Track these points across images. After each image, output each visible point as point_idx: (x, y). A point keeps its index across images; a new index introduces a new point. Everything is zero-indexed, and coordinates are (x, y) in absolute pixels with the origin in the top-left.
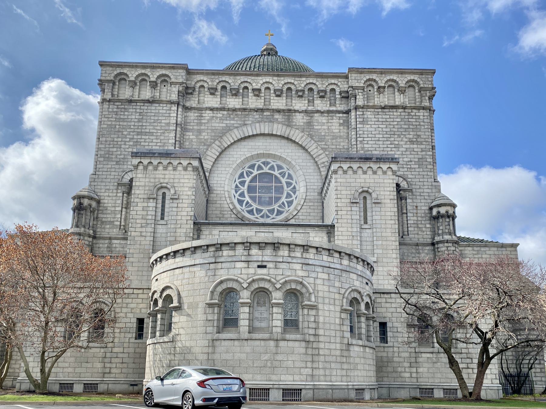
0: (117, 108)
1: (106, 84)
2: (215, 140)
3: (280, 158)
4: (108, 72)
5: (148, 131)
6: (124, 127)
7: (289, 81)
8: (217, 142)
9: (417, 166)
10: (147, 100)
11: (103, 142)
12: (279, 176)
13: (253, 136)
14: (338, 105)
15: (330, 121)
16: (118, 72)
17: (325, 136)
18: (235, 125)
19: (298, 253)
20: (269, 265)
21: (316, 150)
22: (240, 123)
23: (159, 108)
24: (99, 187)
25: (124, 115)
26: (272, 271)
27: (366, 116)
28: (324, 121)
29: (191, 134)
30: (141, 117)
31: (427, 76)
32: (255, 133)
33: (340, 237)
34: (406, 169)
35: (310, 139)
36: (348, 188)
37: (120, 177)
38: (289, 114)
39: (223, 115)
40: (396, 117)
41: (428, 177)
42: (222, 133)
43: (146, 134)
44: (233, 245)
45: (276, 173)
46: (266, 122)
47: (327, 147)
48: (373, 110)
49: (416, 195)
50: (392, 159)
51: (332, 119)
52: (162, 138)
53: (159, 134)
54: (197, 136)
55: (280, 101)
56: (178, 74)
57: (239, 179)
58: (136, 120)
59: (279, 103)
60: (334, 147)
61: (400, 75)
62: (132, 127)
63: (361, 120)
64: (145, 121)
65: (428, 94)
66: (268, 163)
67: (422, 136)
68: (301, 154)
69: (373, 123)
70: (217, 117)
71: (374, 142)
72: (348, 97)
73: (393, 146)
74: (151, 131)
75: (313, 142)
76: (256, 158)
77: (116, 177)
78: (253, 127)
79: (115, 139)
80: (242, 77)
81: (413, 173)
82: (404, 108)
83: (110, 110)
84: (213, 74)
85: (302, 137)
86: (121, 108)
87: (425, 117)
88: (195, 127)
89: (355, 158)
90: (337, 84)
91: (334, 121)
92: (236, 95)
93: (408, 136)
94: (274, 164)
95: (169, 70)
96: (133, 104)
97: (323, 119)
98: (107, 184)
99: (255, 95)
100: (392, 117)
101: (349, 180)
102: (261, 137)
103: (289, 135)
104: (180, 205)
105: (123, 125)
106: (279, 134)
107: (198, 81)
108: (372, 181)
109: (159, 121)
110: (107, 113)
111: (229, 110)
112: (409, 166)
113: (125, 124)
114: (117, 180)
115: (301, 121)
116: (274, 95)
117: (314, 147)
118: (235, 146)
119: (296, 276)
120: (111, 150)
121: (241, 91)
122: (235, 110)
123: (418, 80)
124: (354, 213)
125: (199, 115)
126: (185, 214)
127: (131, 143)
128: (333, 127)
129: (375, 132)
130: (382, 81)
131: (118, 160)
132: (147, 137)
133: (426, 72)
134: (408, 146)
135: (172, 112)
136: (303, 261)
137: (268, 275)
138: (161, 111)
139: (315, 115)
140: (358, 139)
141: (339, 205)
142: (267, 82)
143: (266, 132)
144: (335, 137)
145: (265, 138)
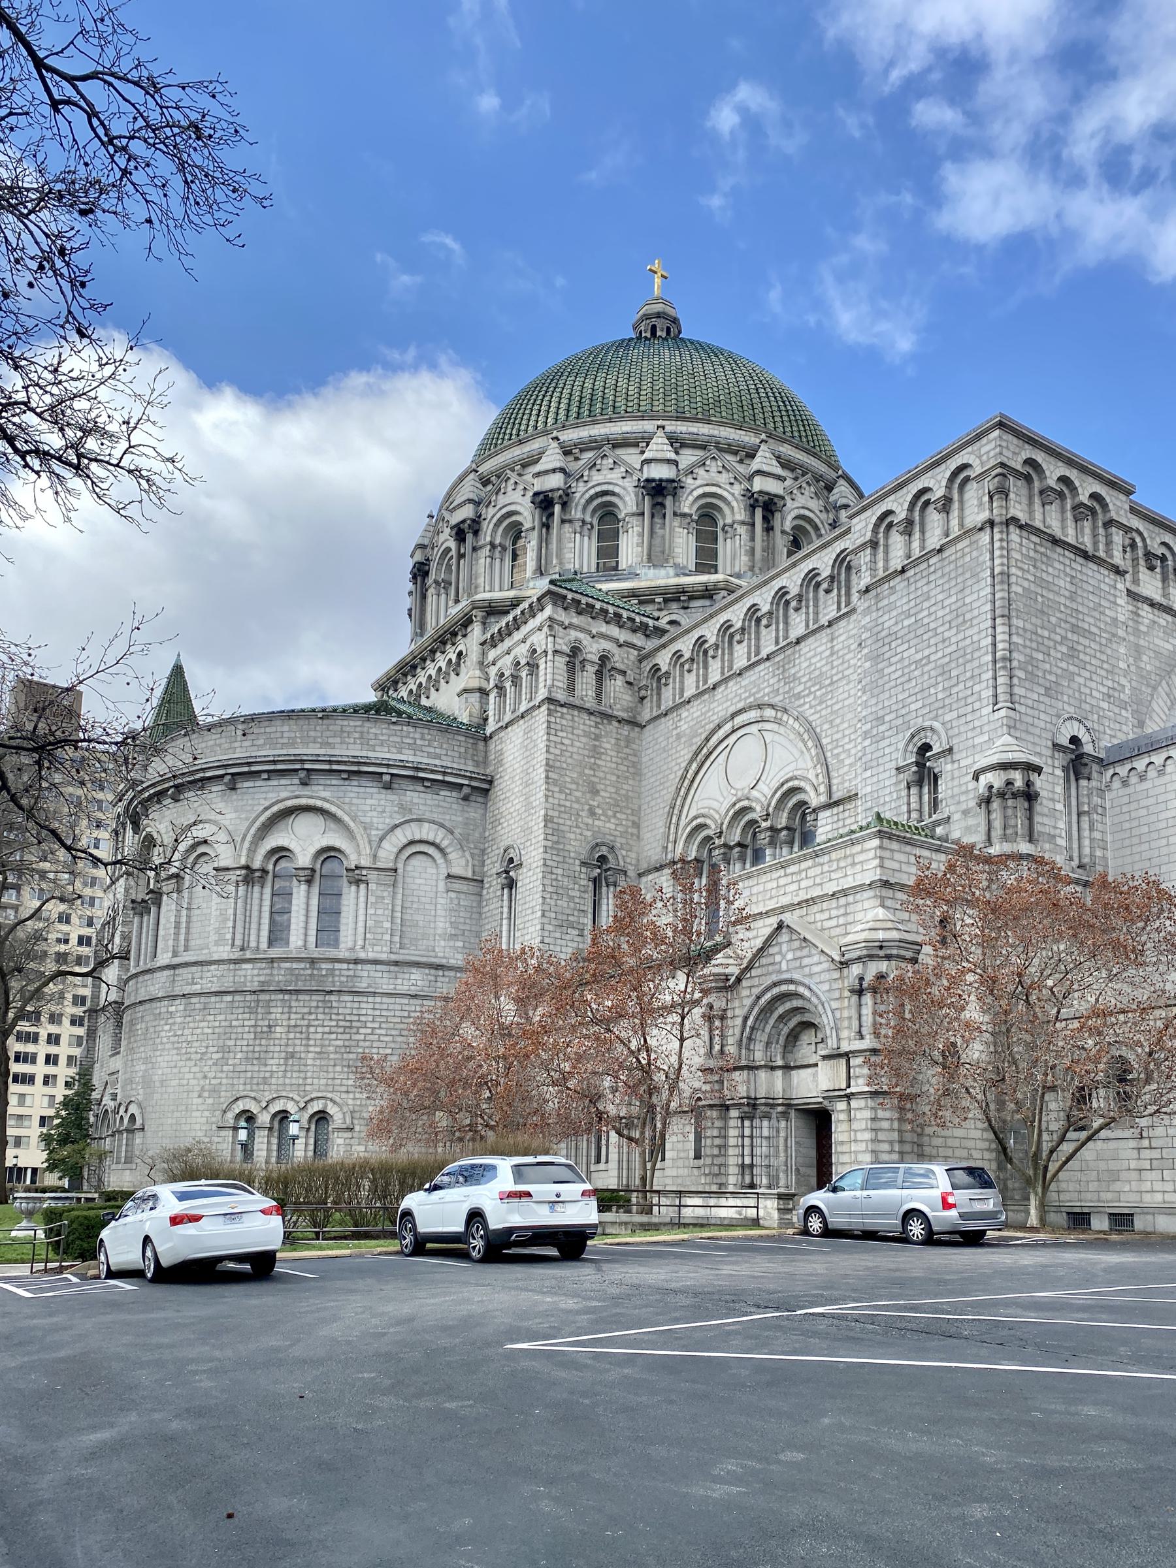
4: (1012, 448)
5: (1086, 626)
11: (1021, 632)
54: (1135, 659)
58: (1067, 594)
62: (1062, 609)
70: (1159, 625)
74: (1094, 629)
98: (1037, 740)
105: (1049, 599)
110: (1019, 557)
113: (1051, 596)
114: (1049, 736)
120: (1035, 655)
132: (1087, 642)
138: (1102, 586)
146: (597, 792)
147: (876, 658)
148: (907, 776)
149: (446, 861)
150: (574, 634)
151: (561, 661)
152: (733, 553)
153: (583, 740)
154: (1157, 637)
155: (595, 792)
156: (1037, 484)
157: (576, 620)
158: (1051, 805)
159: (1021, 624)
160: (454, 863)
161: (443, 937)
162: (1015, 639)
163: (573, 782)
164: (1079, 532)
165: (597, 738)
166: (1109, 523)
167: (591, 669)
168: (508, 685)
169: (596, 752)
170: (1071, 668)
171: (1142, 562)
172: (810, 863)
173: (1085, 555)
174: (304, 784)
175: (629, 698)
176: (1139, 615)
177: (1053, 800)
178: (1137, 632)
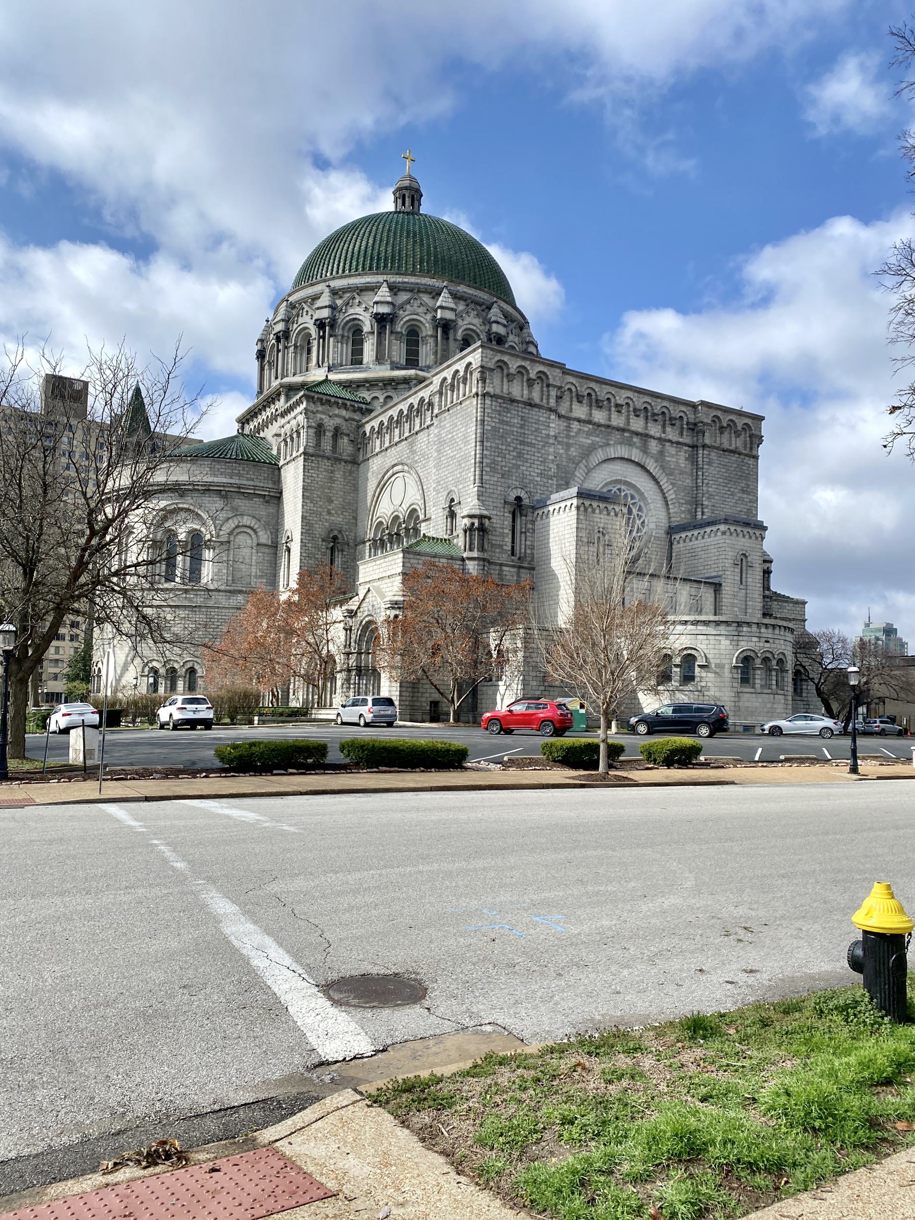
2: (583, 458)
3: (634, 487)
4: (489, 356)
5: (529, 441)
8: (584, 461)
13: (615, 458)
18: (600, 444)
21: (666, 485)
28: (674, 453)
29: (560, 447)
59: (637, 424)
72: (693, 430)
74: (534, 441)
84: (582, 378)
110: (490, 411)
111: (594, 424)
120: (496, 459)
122: (599, 425)
127: (515, 454)
138: (541, 419)
139: (668, 444)
140: (705, 481)
144: (682, 473)
146: (332, 501)
147: (438, 451)
148: (446, 512)
149: (257, 536)
150: (319, 416)
151: (312, 431)
152: (426, 353)
153: (324, 473)
155: (330, 501)
156: (505, 371)
157: (320, 409)
158: (501, 531)
159: (489, 444)
160: (261, 537)
161: (256, 577)
162: (485, 452)
163: (318, 496)
164: (530, 392)
165: (332, 472)
166: (548, 386)
167: (329, 434)
168: (288, 440)
169: (332, 480)
170: (519, 463)
171: (575, 399)
172: (382, 561)
173: (530, 404)
174: (181, 496)
175: (351, 448)
177: (503, 528)
178: (568, 437)
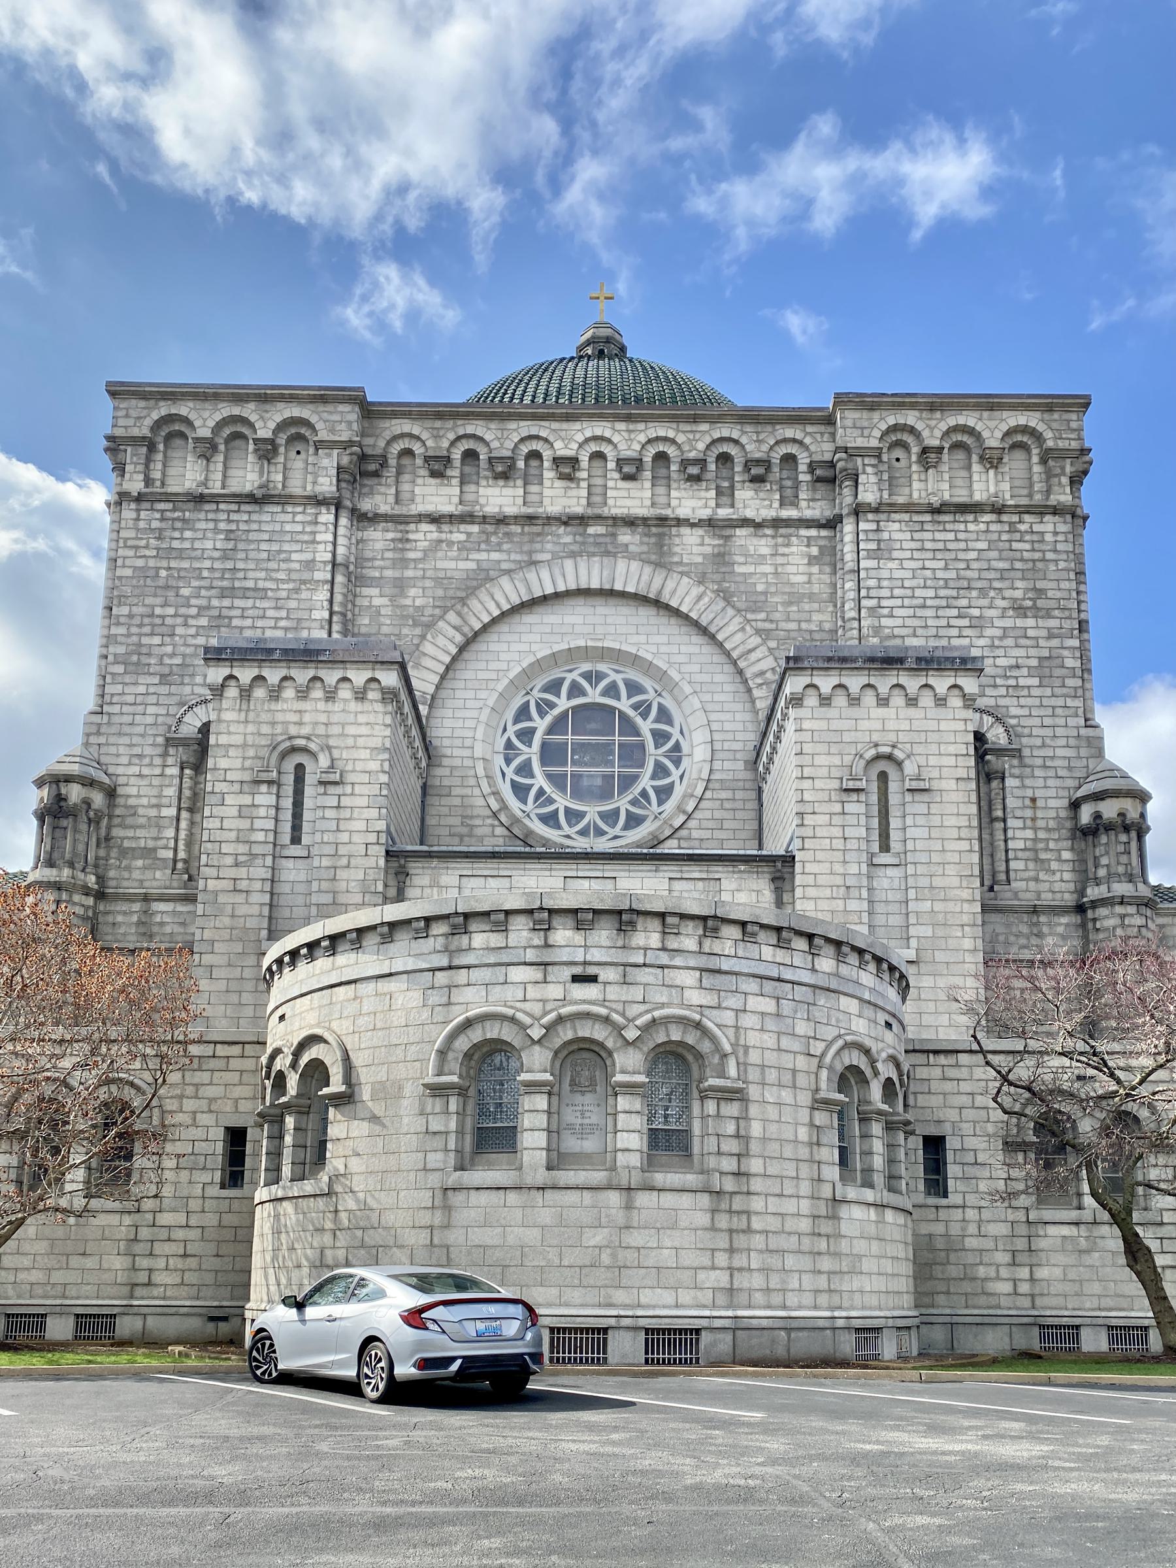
0: (162, 519)
1: (129, 449)
2: (445, 610)
3: (635, 660)
4: (133, 413)
6: (182, 574)
7: (662, 433)
8: (451, 616)
9: (1036, 681)
10: (247, 496)
11: (122, 620)
12: (631, 713)
13: (557, 596)
14: (803, 504)
15: (782, 550)
16: (164, 412)
17: (765, 593)
18: (504, 566)
19: (688, 940)
20: (605, 974)
21: (739, 637)
22: (518, 557)
23: (283, 517)
24: (113, 750)
25: (182, 539)
26: (613, 993)
27: (886, 536)
28: (765, 551)
29: (375, 591)
30: (231, 545)
31: (1066, 416)
32: (561, 588)
33: (811, 892)
34: (1003, 691)
35: (722, 604)
36: (834, 749)
37: (172, 721)
38: (660, 530)
39: (469, 534)
40: (974, 536)
41: (1067, 712)
42: (468, 588)
43: (245, 593)
44: (502, 916)
45: (624, 705)
46: (594, 554)
47: (773, 626)
48: (906, 517)
49: (1032, 767)
50: (964, 661)
51: (788, 545)
52: (293, 604)
53: (284, 594)
54: (392, 598)
55: (633, 493)
56: (337, 417)
57: (515, 722)
58: (217, 554)
59: (630, 499)
60: (793, 626)
61: (986, 414)
62: (205, 574)
63: (873, 546)
64: (242, 555)
65: (1068, 469)
66: (600, 676)
67: (1050, 594)
68: (696, 649)
69: (908, 554)
70: (450, 543)
71: (911, 612)
72: (832, 481)
73: (966, 622)
74: (261, 584)
75: (730, 612)
76: (566, 663)
77: (160, 720)
78: (557, 571)
79: (158, 611)
80: (522, 423)
81: (1023, 701)
82: (999, 510)
83: (142, 524)
85: (700, 598)
86: (174, 519)
87: (1060, 538)
88: (388, 573)
89: (855, 660)
90: (800, 443)
91: (794, 549)
92: (505, 476)
93: (1007, 593)
94: (619, 679)
95: (310, 406)
96: (207, 507)
97: (762, 545)
98: (135, 740)
99: (562, 477)
100: (961, 536)
101: (835, 725)
102: (580, 601)
103: (660, 592)
104: (345, 801)
106: (631, 589)
107: (395, 438)
108: (905, 725)
109: (283, 556)
110: (131, 534)
111: (484, 520)
112: (1012, 682)
113: (185, 564)
114: (162, 730)
115: (695, 550)
116: (616, 475)
117: (733, 627)
118: (504, 627)
119: (682, 1005)
121: (521, 464)
122: (502, 520)
123: (1041, 427)
124: (852, 820)
125: (399, 535)
126: (360, 825)
127: (204, 622)
128: (791, 569)
129: (914, 583)
130: (933, 429)
131: (166, 670)
132: (250, 603)
133: (1064, 405)
134: (1008, 623)
135: (321, 528)
136: (702, 961)
137: (603, 1002)
138: (288, 527)
139: (738, 532)
140: (864, 603)
141: (807, 797)
142: (595, 438)
143: (595, 584)
144: (794, 598)
145: (591, 601)
154: (446, 558)
176: (408, 540)
